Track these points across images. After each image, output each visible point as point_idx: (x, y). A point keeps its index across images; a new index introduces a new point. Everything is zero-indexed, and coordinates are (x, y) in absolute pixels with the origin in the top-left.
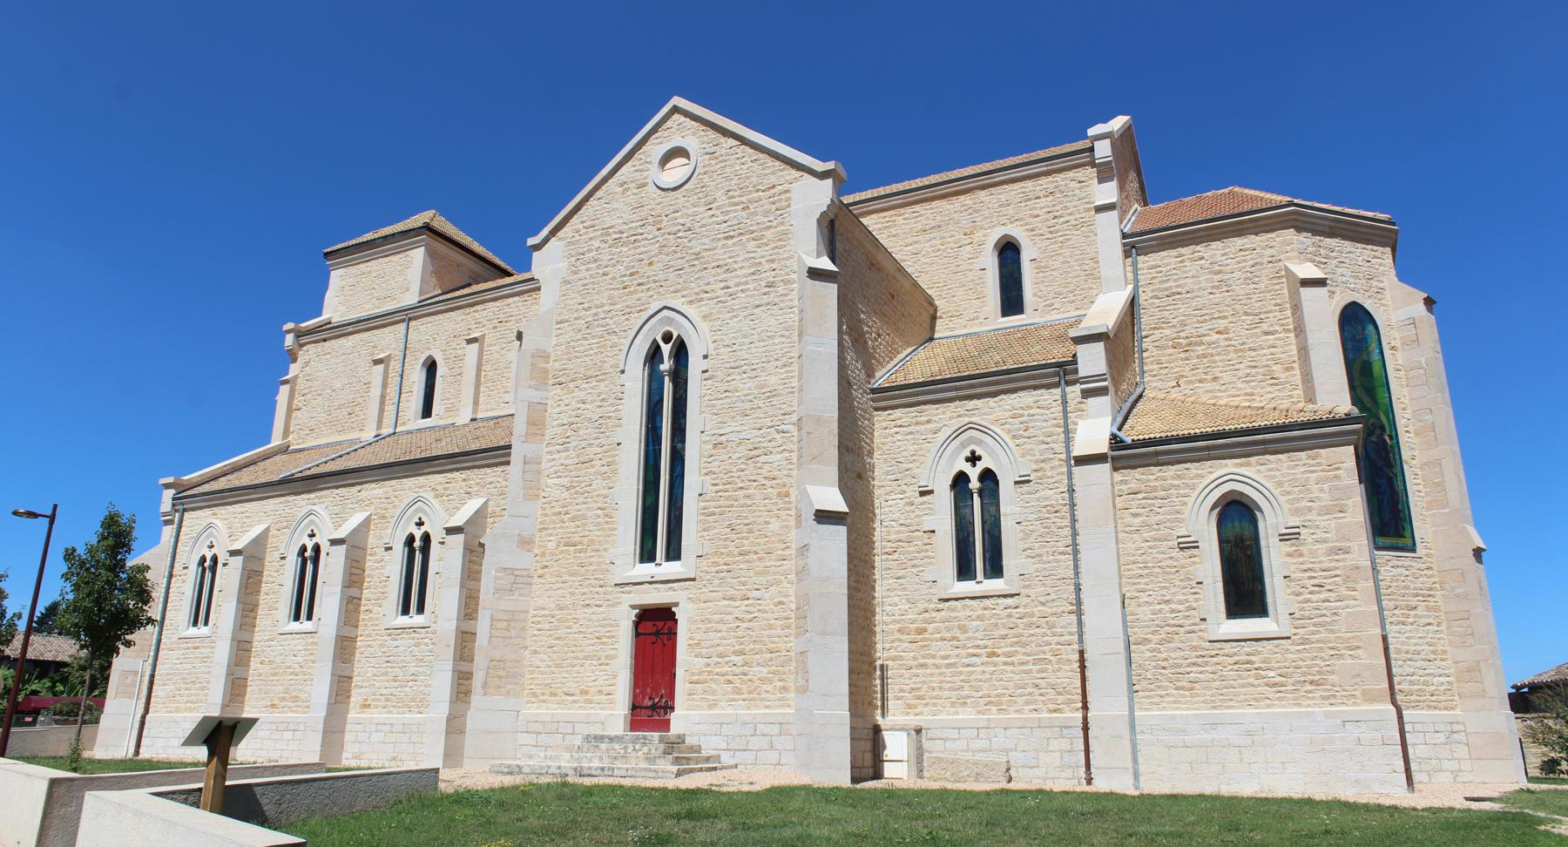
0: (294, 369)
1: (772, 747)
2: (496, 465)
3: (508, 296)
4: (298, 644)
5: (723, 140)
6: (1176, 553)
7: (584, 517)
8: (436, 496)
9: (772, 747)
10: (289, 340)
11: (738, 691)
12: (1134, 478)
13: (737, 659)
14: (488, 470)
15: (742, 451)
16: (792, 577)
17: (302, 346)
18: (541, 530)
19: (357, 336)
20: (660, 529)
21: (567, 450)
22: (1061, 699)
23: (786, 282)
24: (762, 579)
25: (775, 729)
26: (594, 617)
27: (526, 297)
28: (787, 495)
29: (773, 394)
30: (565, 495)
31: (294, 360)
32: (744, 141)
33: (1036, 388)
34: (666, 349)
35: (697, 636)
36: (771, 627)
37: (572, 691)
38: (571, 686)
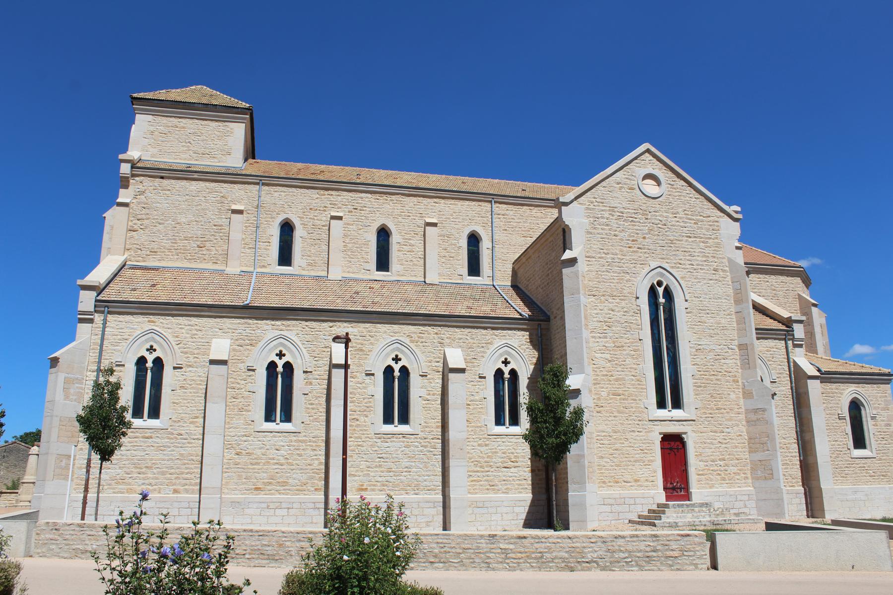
0: (124, 196)
1: (745, 506)
2: (464, 327)
3: (362, 192)
4: (279, 440)
5: (676, 179)
6: (838, 421)
7: (623, 379)
8: (412, 342)
9: (745, 506)
10: (125, 169)
11: (724, 479)
12: (829, 386)
13: (722, 463)
14: (457, 330)
15: (711, 356)
16: (744, 423)
17: (133, 176)
18: (595, 384)
20: (669, 392)
21: (606, 337)
22: (794, 481)
24: (730, 423)
25: (746, 498)
26: (638, 438)
28: (738, 382)
29: (724, 328)
30: (608, 365)
31: (126, 187)
32: (690, 185)
33: (775, 339)
34: (661, 290)
35: (701, 450)
36: (736, 447)
38: (628, 477)
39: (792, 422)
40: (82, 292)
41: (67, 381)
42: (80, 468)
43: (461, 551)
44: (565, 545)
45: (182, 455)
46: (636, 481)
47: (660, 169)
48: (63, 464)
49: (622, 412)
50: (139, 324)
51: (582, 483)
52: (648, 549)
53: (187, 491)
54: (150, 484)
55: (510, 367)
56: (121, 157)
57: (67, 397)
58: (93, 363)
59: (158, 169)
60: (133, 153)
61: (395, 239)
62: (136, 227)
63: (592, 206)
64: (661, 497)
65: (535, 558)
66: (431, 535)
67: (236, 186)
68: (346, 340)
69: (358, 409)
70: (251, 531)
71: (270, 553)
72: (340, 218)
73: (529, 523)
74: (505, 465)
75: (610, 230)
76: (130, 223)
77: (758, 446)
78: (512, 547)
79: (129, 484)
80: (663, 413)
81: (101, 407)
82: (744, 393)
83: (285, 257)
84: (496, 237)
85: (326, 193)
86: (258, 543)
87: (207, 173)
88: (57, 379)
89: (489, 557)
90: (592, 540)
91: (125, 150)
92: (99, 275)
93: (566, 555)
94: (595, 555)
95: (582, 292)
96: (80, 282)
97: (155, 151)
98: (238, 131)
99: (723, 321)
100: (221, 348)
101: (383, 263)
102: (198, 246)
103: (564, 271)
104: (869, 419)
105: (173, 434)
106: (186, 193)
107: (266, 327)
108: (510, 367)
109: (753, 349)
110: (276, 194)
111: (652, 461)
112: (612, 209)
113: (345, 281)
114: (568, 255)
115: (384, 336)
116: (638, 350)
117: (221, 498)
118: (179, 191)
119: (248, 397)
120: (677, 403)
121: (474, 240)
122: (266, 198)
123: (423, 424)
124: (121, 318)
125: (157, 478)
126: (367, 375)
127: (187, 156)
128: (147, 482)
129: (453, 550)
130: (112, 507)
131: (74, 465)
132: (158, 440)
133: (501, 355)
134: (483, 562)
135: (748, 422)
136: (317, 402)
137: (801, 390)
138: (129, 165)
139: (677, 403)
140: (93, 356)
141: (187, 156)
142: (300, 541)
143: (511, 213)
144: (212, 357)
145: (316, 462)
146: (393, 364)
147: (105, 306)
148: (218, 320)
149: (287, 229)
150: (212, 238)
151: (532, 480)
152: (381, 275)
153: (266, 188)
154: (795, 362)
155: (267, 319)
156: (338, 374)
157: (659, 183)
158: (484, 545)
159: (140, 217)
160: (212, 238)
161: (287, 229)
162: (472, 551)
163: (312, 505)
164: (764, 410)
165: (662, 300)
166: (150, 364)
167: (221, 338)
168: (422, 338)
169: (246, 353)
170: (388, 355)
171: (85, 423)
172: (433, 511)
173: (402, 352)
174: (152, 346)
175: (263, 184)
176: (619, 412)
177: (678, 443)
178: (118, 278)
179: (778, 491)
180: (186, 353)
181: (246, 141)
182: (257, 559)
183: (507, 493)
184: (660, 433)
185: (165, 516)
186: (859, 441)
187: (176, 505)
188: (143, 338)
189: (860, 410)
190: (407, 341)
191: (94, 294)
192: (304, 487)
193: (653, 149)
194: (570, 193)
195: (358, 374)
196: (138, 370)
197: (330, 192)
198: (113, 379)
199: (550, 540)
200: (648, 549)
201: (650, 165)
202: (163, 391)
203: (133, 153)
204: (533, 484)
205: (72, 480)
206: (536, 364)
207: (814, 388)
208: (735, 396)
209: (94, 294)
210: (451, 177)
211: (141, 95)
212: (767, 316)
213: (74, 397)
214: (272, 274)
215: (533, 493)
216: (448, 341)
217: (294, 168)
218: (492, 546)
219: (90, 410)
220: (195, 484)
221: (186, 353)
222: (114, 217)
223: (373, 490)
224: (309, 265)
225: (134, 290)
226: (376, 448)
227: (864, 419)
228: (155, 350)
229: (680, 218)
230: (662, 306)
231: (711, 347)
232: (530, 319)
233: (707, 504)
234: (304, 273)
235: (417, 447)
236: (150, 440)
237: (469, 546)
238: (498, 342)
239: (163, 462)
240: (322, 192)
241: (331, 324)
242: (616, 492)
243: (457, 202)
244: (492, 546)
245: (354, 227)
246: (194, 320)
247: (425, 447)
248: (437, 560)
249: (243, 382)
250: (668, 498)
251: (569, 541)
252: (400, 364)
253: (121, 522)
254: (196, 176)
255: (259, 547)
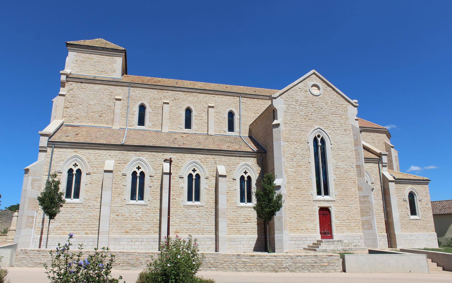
0: (62, 91)
1: (359, 242)
2: (226, 156)
4: (138, 209)
5: (327, 87)
6: (403, 202)
7: (301, 181)
8: (202, 162)
9: (359, 242)
10: (63, 78)
11: (349, 229)
13: (348, 221)
14: (223, 157)
15: (343, 170)
16: (358, 202)
17: (67, 81)
18: (288, 183)
19: (101, 86)
20: (323, 187)
21: (293, 161)
23: (349, 130)
24: (352, 202)
27: (186, 93)
29: (349, 158)
32: (334, 90)
33: (373, 163)
34: (319, 139)
35: (338, 215)
37: (303, 229)
38: (303, 228)
39: (381, 202)
40: (41, 137)
41: (33, 180)
42: (39, 223)
43: (223, 262)
44: (273, 260)
45: (90, 216)
46: (307, 229)
47: (320, 82)
48: (30, 221)
49: (301, 197)
50: (70, 153)
51: (281, 230)
52: (313, 262)
53: (92, 233)
54: (74, 230)
55: (247, 175)
56: (61, 72)
57: (33, 188)
58: (46, 171)
59: (80, 78)
60: (67, 70)
61: (194, 114)
62: (68, 106)
63: (287, 99)
64: (319, 237)
65: (259, 266)
66: (210, 254)
67: (118, 87)
68: (170, 161)
69: (176, 194)
70: (123, 252)
71: (132, 263)
72: (168, 103)
73: (256, 250)
74: (245, 221)
75: (295, 110)
76: (66, 104)
77: (365, 213)
78: (248, 260)
79: (63, 230)
80: (320, 197)
81: (50, 193)
82: (359, 188)
83: (141, 122)
84: (241, 113)
85: (161, 91)
86: (126, 258)
87: (104, 81)
88: (28, 180)
89: (237, 265)
90: (286, 257)
91: (63, 69)
92: (50, 129)
93: (274, 265)
94: (287, 265)
95: (282, 140)
96: (40, 132)
97: (78, 70)
98: (119, 61)
99: (349, 154)
100: (110, 164)
101: (188, 125)
102: (99, 116)
103: (274, 130)
104: (418, 201)
105: (85, 206)
106: (92, 90)
107: (131, 155)
108: (247, 175)
109: (363, 167)
110: (137, 92)
111: (315, 220)
112: (297, 101)
113: (170, 133)
114: (275, 122)
115: (189, 159)
116: (308, 167)
117: (109, 237)
118: (90, 89)
119: (123, 188)
120: (327, 193)
121: (231, 115)
122: (132, 93)
123: (207, 201)
124: (61, 150)
125: (77, 227)
126: (180, 178)
127: (94, 72)
128: (72, 229)
129: (220, 261)
130: (55, 242)
131: (36, 221)
132: (78, 209)
133: (243, 169)
134: (234, 268)
135: (360, 202)
136: (156, 190)
137: (386, 187)
138: (65, 76)
139: (327, 193)
140: (47, 168)
141: (94, 72)
142: (147, 257)
143: (249, 102)
144: (105, 169)
145: (155, 219)
146: (192, 173)
147: (53, 144)
148: (108, 151)
149: (142, 108)
150: (106, 112)
151: (258, 228)
152: (187, 131)
153: (133, 88)
154: (383, 174)
155: (132, 151)
156: (166, 177)
157: (319, 89)
158: (234, 259)
159: (70, 101)
160: (106, 112)
161: (142, 108)
162: (229, 262)
163: (153, 240)
164: (368, 196)
165: (320, 144)
166: (75, 172)
167: (110, 160)
168: (206, 160)
169: (122, 167)
170: (190, 168)
171: (42, 201)
172: (211, 243)
173: (197, 167)
174: (76, 164)
175: (131, 87)
176: (299, 197)
177: (327, 212)
178: (59, 131)
179: (375, 235)
180: (93, 167)
181: (123, 66)
182: (126, 266)
183: (246, 235)
184: (319, 207)
185: (81, 246)
186: (413, 212)
187: (86, 240)
188: (72, 160)
189: (414, 197)
190: (199, 162)
191: (47, 138)
192: (149, 231)
193: (317, 73)
194: (277, 93)
195: (176, 178)
196: (69, 175)
197: (163, 91)
198: (56, 179)
199: (266, 257)
200: (313, 262)
201: (315, 80)
202: (81, 185)
203: (67, 70)
204: (258, 231)
205: (35, 229)
206: (260, 174)
207: (392, 186)
208: (354, 189)
209: (47, 138)
210: (221, 85)
211: (71, 42)
212: (370, 152)
213: (37, 188)
214: (135, 130)
215: (258, 235)
216: (218, 162)
217: (146, 79)
218: (239, 260)
219: (45, 194)
220: (96, 230)
221: (93, 167)
222: (58, 101)
223: (182, 233)
224: (153, 125)
225: (67, 136)
226: (184, 213)
227: (416, 201)
228: (77, 165)
229: (329, 105)
230: (320, 146)
231: (343, 166)
232: (257, 152)
233: (341, 241)
234: (150, 129)
235: (203, 212)
236: (74, 209)
237: (228, 260)
238: (242, 163)
239: (80, 220)
240: (159, 91)
241: (163, 154)
242: (297, 234)
243: (223, 96)
244: (239, 260)
245: (174, 108)
246: (97, 151)
247: (207, 212)
248: (212, 266)
249: (120, 181)
250: (322, 238)
251: (275, 258)
252: (196, 173)
253: (59, 249)
254: (98, 82)
255: (127, 260)
